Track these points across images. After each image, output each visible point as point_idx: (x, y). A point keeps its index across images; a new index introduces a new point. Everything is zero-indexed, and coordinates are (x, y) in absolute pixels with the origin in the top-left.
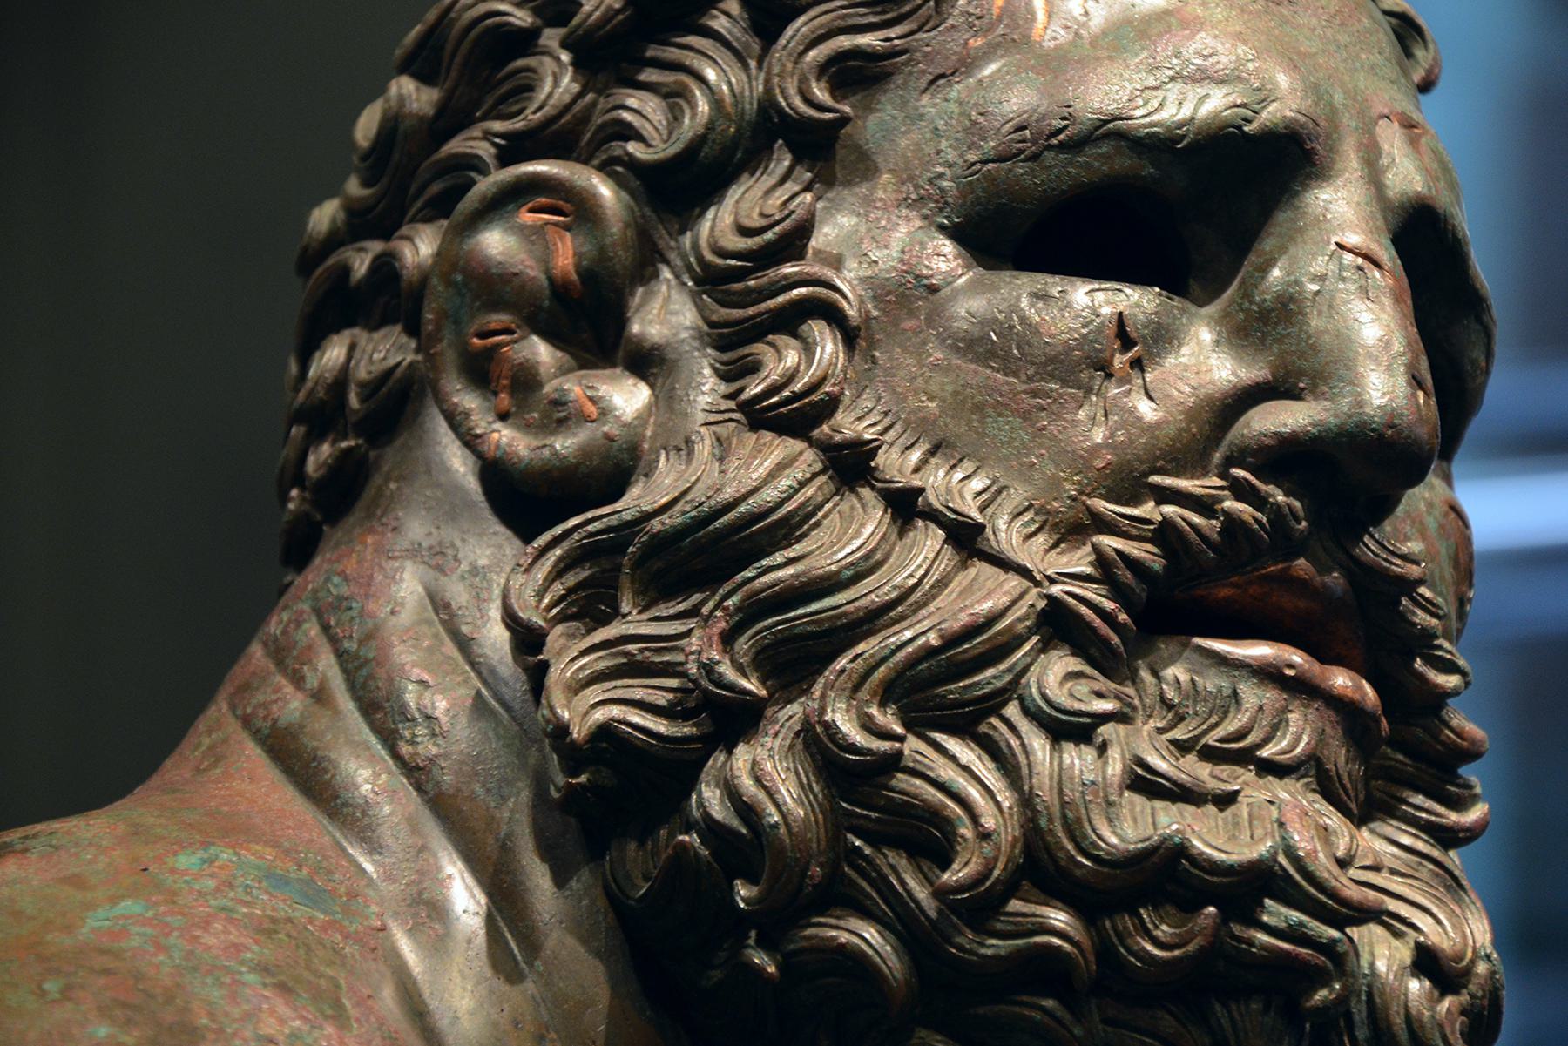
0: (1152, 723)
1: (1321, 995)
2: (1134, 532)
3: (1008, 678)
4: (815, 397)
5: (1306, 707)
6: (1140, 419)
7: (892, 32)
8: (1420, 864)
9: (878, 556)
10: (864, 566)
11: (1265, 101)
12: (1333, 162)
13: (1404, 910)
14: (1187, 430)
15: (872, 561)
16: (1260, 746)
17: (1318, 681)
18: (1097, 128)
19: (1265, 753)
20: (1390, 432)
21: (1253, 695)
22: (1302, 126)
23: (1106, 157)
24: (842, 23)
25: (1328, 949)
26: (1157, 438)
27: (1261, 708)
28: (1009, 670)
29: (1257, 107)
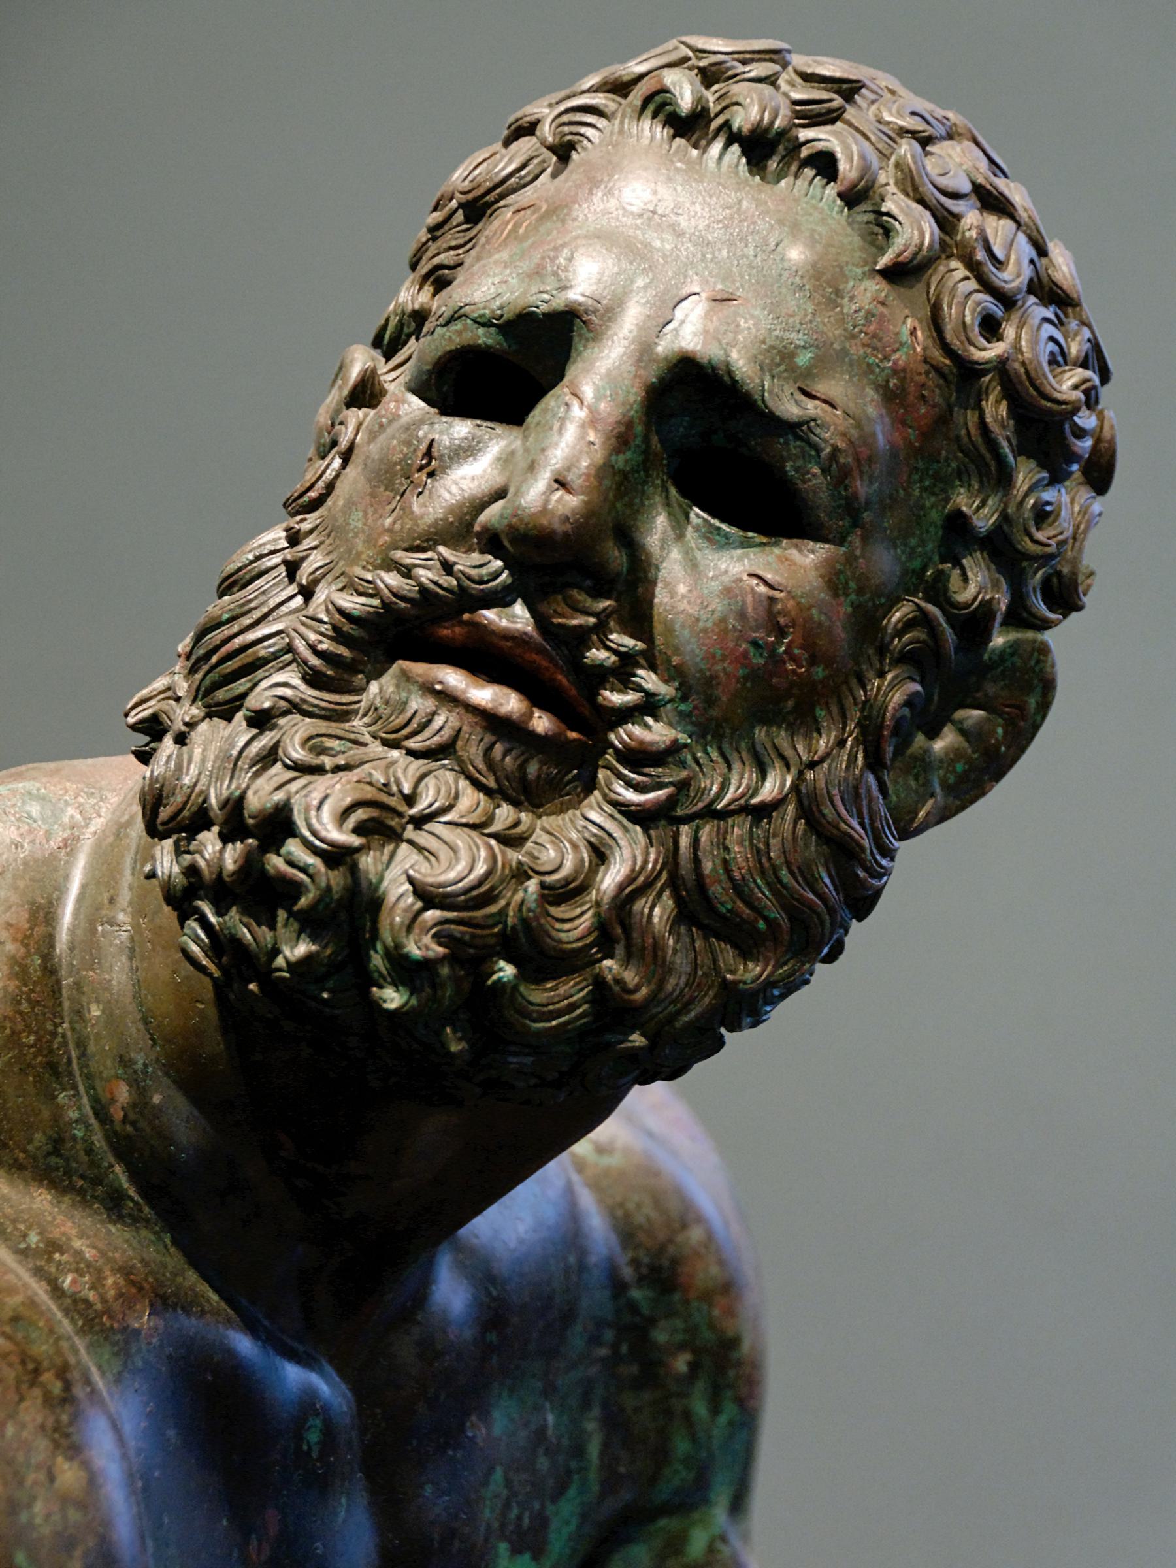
0: (366, 720)
1: (303, 902)
2: (361, 589)
3: (249, 685)
4: (301, 501)
5: (450, 711)
6: (412, 512)
7: (460, 251)
8: (585, 827)
9: (253, 605)
10: (238, 611)
11: (564, 288)
12: (608, 328)
13: (444, 853)
14: (445, 519)
15: (246, 608)
16: (407, 737)
17: (459, 694)
18: (456, 312)
19: (411, 744)
20: (514, 520)
21: (419, 704)
22: (580, 305)
23: (459, 333)
24: (445, 246)
25: (304, 869)
26: (418, 525)
27: (416, 712)
28: (250, 681)
29: (554, 292)
